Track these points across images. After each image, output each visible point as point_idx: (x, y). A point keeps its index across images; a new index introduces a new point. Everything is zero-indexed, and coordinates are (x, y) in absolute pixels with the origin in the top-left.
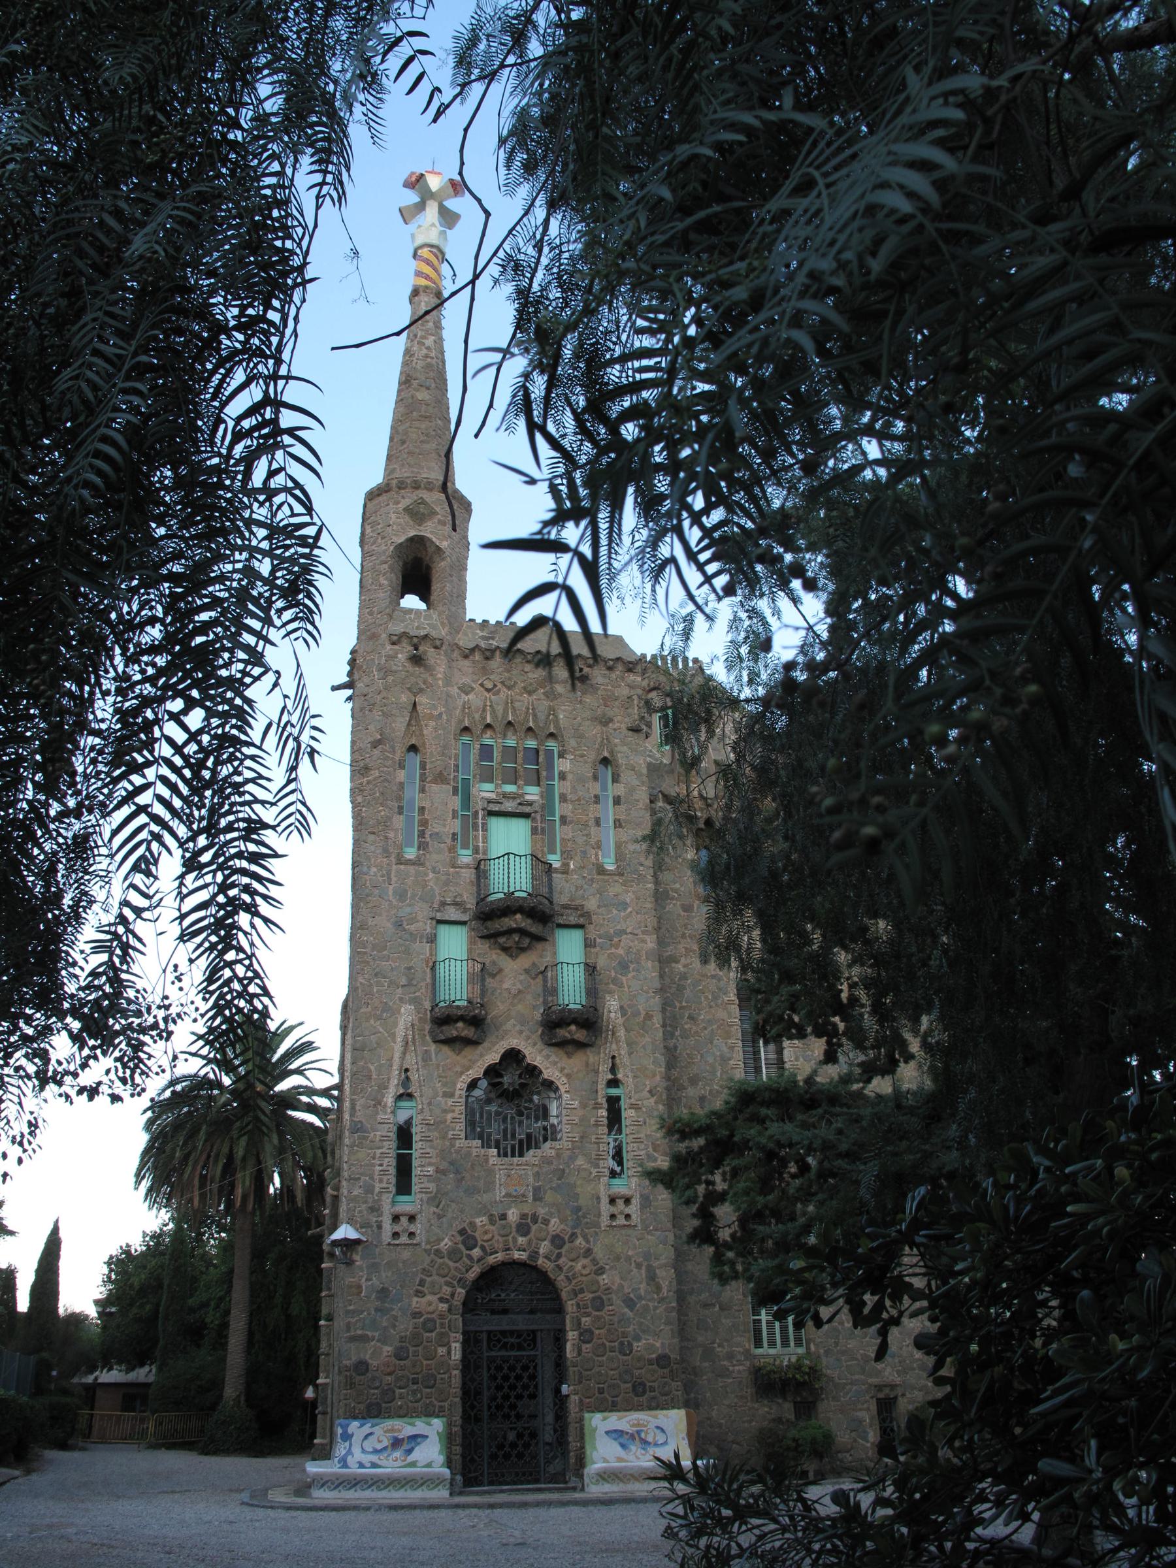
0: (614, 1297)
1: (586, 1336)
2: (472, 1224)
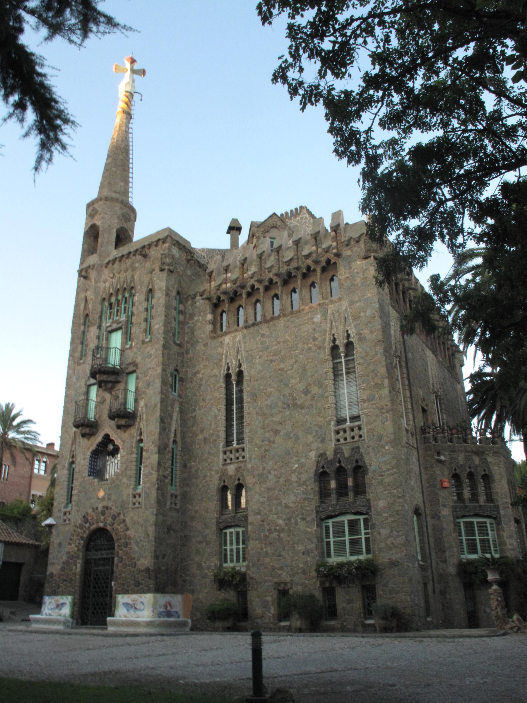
0: (132, 541)
2: (87, 513)
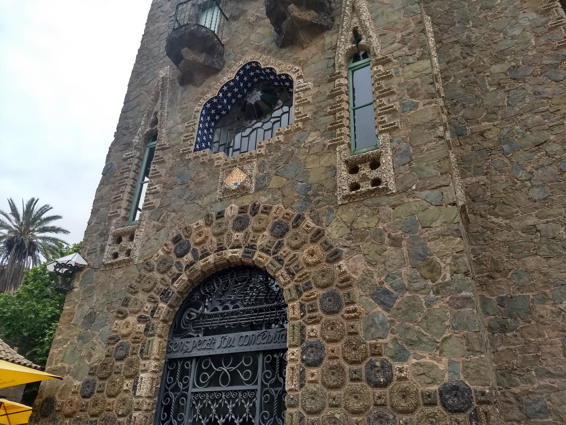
0: (357, 291)
1: (314, 356)
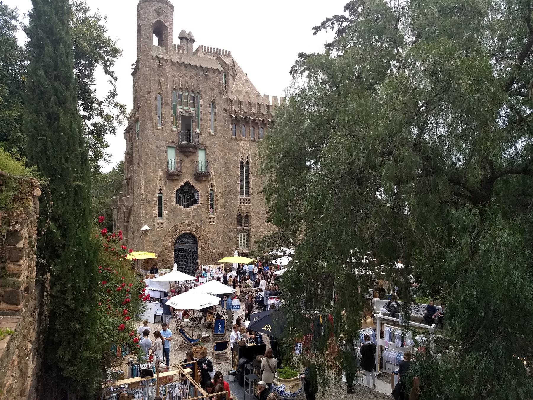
1: (203, 249)
